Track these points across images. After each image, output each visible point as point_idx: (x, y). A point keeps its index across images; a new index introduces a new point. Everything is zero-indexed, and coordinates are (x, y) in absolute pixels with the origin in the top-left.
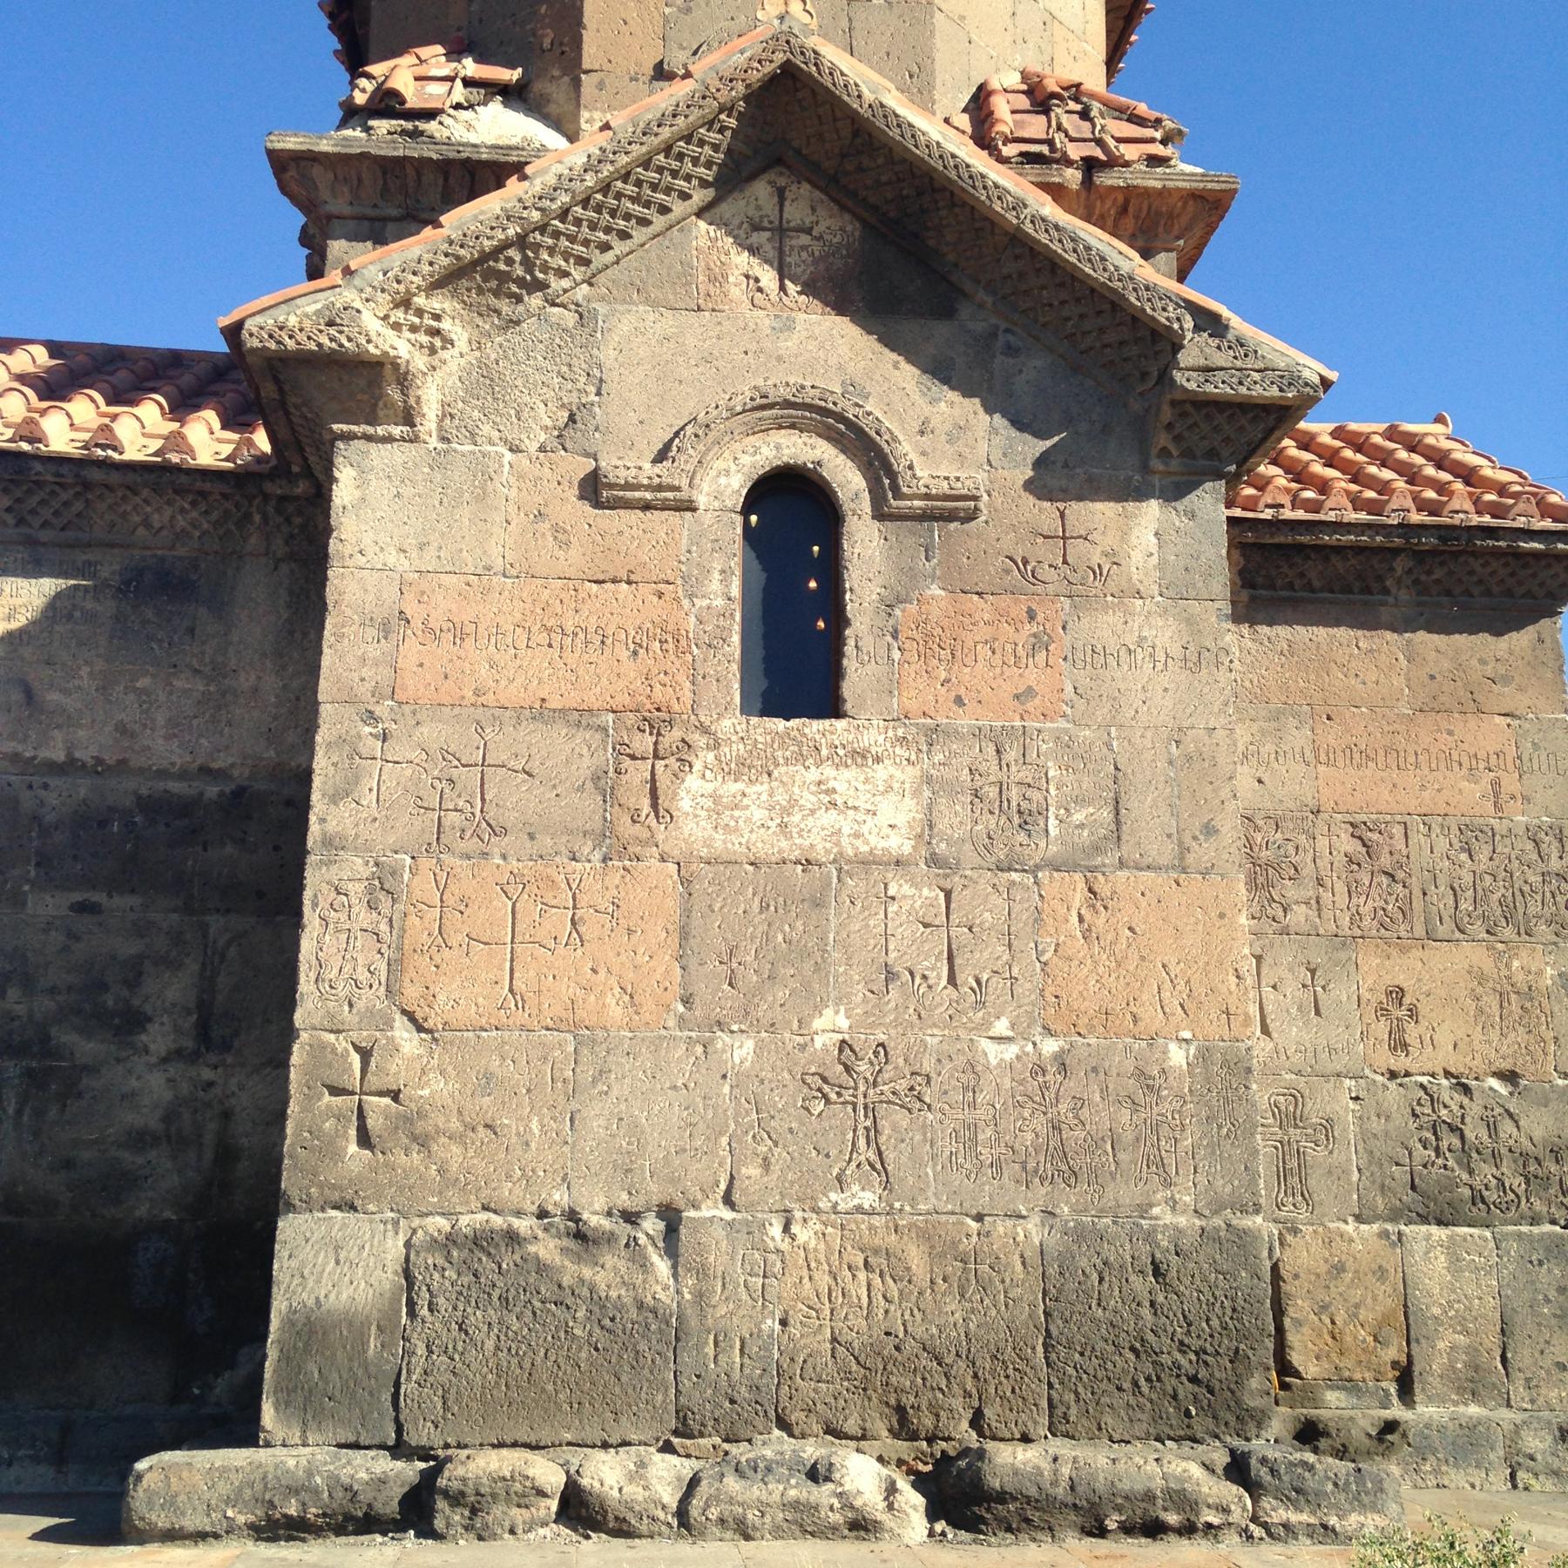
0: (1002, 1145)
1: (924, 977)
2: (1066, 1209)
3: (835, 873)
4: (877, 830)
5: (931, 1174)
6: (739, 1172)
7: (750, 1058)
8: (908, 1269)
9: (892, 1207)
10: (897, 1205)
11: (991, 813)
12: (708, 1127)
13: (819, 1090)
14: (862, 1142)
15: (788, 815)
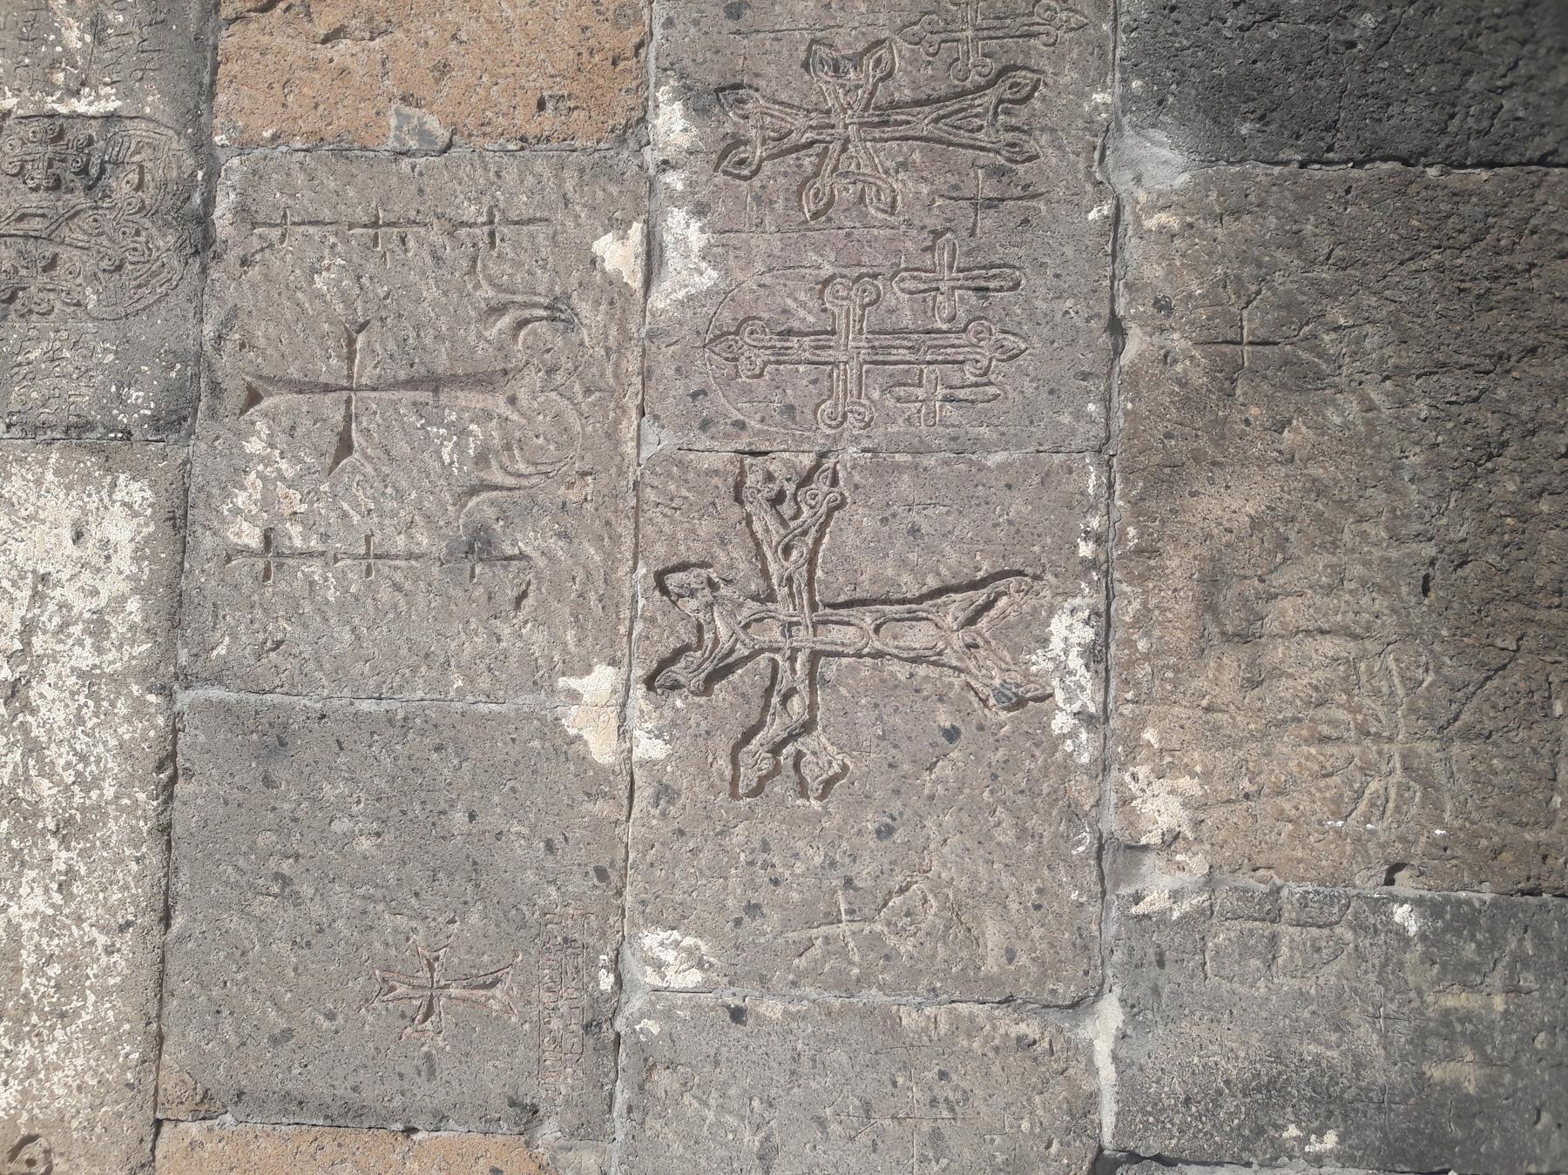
0: (928, 260)
1: (482, 459)
2: (1098, 97)
3: (200, 693)
4: (86, 576)
5: (1000, 457)
6: (993, 982)
7: (689, 941)
8: (1256, 524)
9: (1092, 564)
10: (1086, 550)
11: (52, 264)
12: (873, 1065)
13: (776, 750)
14: (919, 637)
15: (37, 814)
